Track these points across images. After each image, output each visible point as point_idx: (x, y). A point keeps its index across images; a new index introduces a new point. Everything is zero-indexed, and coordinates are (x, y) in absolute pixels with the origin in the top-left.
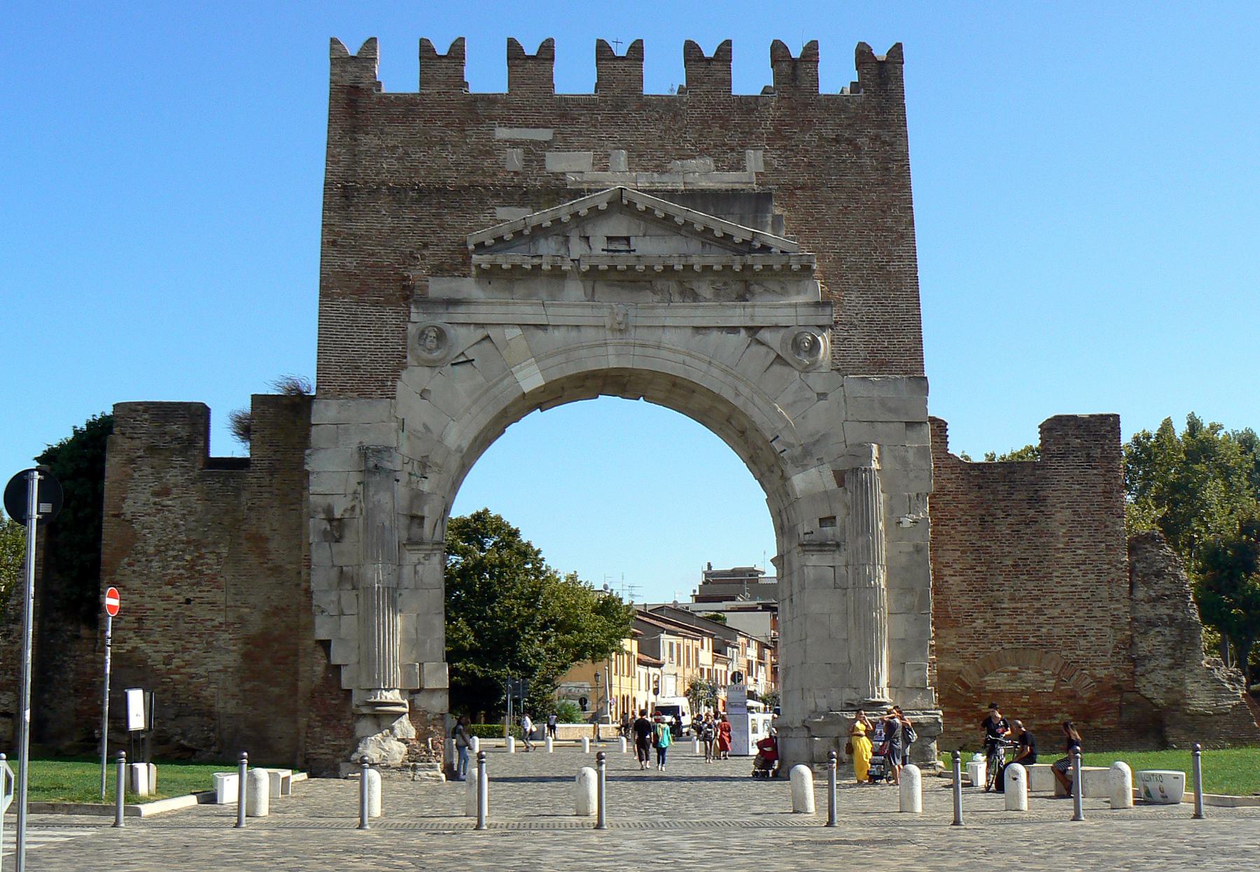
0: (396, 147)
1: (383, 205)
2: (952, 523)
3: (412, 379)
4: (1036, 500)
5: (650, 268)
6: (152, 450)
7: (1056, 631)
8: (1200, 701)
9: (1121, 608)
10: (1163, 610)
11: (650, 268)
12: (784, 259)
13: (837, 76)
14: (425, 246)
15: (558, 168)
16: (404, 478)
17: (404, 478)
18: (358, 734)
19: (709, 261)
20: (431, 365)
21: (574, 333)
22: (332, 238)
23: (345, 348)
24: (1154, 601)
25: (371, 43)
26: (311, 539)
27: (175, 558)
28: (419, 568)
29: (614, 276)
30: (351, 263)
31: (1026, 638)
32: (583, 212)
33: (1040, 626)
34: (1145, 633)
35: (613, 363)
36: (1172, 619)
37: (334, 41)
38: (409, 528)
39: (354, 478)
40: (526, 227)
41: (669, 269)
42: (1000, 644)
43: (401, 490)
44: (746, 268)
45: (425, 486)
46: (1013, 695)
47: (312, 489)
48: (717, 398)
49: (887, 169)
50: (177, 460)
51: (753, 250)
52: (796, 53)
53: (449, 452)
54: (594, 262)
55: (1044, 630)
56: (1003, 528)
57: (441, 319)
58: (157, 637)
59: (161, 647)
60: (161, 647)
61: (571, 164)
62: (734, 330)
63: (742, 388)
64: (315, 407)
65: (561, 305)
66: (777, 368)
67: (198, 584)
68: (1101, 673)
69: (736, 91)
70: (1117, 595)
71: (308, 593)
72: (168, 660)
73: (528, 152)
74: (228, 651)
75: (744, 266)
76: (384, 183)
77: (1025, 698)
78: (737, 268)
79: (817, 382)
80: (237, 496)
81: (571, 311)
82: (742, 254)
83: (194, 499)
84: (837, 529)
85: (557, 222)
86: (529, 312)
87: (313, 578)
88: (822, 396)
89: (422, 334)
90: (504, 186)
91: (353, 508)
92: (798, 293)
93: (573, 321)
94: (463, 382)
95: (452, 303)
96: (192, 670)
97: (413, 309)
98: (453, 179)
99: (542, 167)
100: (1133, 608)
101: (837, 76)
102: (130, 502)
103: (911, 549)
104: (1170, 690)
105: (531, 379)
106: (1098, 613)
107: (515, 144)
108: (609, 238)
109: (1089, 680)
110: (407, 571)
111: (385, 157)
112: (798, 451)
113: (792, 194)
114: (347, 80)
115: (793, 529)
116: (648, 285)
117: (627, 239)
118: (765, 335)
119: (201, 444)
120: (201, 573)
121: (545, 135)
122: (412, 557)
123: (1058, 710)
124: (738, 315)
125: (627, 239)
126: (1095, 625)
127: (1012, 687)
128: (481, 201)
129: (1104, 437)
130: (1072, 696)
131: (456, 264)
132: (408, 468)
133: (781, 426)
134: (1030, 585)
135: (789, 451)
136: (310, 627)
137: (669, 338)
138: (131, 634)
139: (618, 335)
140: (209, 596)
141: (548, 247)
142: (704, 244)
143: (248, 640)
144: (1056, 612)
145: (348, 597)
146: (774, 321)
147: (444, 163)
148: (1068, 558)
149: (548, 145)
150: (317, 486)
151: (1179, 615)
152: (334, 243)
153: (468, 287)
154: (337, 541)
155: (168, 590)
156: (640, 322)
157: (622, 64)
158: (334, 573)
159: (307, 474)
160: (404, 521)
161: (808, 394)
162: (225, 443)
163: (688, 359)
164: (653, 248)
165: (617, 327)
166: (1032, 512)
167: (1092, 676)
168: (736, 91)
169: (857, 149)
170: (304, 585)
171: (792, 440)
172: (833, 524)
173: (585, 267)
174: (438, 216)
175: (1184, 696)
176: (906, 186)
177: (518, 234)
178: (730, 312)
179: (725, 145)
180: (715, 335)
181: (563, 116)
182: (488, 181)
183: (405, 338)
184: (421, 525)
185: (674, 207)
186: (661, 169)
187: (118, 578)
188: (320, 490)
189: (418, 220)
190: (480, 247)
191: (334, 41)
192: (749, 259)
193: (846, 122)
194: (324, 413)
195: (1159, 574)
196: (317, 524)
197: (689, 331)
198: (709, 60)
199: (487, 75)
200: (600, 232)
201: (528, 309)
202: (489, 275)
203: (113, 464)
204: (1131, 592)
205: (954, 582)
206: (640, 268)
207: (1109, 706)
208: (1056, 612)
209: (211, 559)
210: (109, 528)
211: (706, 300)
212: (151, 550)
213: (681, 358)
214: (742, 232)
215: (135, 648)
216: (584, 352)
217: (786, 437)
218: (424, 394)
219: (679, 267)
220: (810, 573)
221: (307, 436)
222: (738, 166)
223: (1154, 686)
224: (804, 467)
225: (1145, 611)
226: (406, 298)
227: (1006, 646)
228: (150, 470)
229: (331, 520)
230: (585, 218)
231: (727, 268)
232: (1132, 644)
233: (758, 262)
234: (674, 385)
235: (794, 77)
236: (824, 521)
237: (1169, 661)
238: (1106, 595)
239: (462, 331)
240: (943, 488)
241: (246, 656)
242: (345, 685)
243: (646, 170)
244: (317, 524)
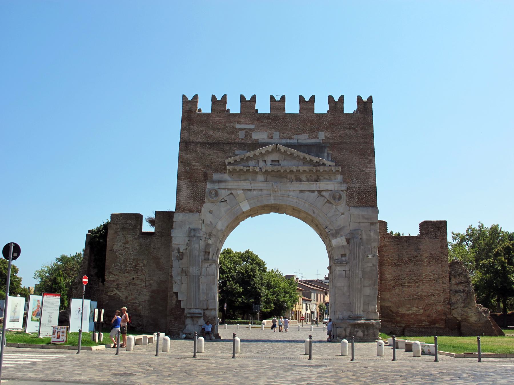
0: (203, 130)
1: (199, 149)
2: (388, 256)
3: (207, 206)
4: (417, 249)
5: (285, 171)
6: (123, 229)
7: (424, 294)
8: (473, 318)
9: (446, 286)
10: (461, 287)
11: (285, 171)
12: (330, 168)
13: (350, 107)
14: (212, 163)
15: (256, 138)
16: (203, 239)
17: (203, 239)
18: (186, 323)
19: (305, 168)
20: (213, 202)
21: (260, 192)
22: (181, 160)
23: (185, 196)
24: (458, 284)
25: (196, 97)
26: (173, 259)
27: (130, 264)
28: (208, 269)
30: (188, 168)
31: (413, 296)
32: (264, 152)
33: (418, 292)
34: (455, 295)
35: (273, 202)
36: (464, 291)
37: (184, 96)
38: (204, 256)
39: (187, 239)
41: (291, 171)
42: (404, 298)
43: (202, 243)
44: (317, 171)
45: (210, 242)
46: (408, 315)
47: (173, 242)
48: (307, 214)
49: (366, 138)
50: (131, 232)
51: (320, 165)
52: (336, 99)
53: (218, 231)
54: (267, 168)
55: (419, 293)
56: (406, 258)
57: (216, 186)
58: (123, 290)
59: (124, 293)
60: (124, 293)
61: (260, 136)
62: (313, 191)
63: (315, 211)
64: (175, 215)
66: (327, 204)
67: (137, 273)
68: (439, 308)
69: (315, 112)
70: (445, 282)
71: (171, 276)
72: (126, 298)
73: (246, 132)
74: (146, 295)
75: (317, 171)
76: (199, 142)
77: (413, 316)
78: (314, 171)
80: (150, 244)
82: (316, 166)
83: (136, 245)
84: (347, 258)
85: (255, 155)
86: (246, 185)
87: (173, 272)
88: (342, 214)
89: (210, 192)
90: (238, 143)
91: (186, 249)
92: (335, 179)
93: (260, 188)
94: (223, 208)
95: (220, 181)
96: (134, 301)
97: (207, 183)
98: (221, 140)
99: (251, 137)
100: (450, 286)
101: (350, 107)
102: (115, 246)
103: (371, 265)
104: (462, 315)
105: (245, 207)
106: (439, 288)
107: (242, 129)
108: (272, 161)
109: (435, 311)
110: (204, 270)
111: (199, 134)
112: (334, 232)
113: (334, 146)
114: (188, 108)
115: (333, 258)
117: (278, 161)
118: (324, 193)
119: (139, 227)
120: (138, 269)
121: (252, 127)
122: (205, 265)
123: (424, 320)
124: (314, 186)
125: (278, 161)
126: (437, 292)
127: (408, 312)
128: (230, 148)
129: (441, 228)
130: (429, 316)
131: (222, 170)
132: (205, 236)
134: (415, 278)
135: (331, 232)
136: (172, 288)
137: (291, 193)
138: (115, 289)
139: (275, 193)
140: (140, 277)
141: (252, 163)
142: (304, 163)
143: (152, 291)
144: (424, 287)
145: (184, 278)
146: (327, 188)
147: (219, 136)
148: (428, 269)
149: (252, 130)
150: (174, 241)
151: (467, 289)
152: (182, 162)
153: (226, 176)
154: (181, 259)
155: (127, 275)
157: (278, 103)
158: (180, 270)
159: (172, 237)
160: (203, 253)
161: (338, 213)
162: (147, 228)
164: (287, 165)
166: (415, 253)
167: (436, 309)
168: (316, 112)
169: (357, 131)
170: (170, 274)
171: (332, 228)
172: (345, 257)
173: (264, 170)
174: (216, 153)
175: (468, 317)
176: (373, 144)
177: (242, 159)
178: (312, 186)
179: (312, 130)
180: (307, 193)
181: (258, 120)
182: (233, 141)
183: (205, 193)
184: (209, 255)
185: (293, 151)
186: (291, 138)
187: (111, 271)
188: (176, 243)
189: (210, 154)
190: (230, 164)
191: (184, 96)
192: (318, 168)
193: (353, 122)
194: (177, 218)
195: (459, 275)
196: (175, 254)
198: (307, 102)
199: (234, 107)
200: (269, 159)
201: (244, 184)
202: (232, 172)
203: (110, 233)
204: (450, 281)
205: (388, 276)
206: (282, 171)
207: (442, 320)
208: (424, 287)
209: (141, 265)
210: (108, 255)
212: (122, 262)
214: (316, 159)
215: (116, 294)
218: (210, 212)
220: (337, 273)
221: (173, 225)
222: (316, 137)
223: (457, 314)
224: (336, 237)
225: (455, 287)
226: (205, 180)
227: (406, 298)
228: (122, 236)
229: (179, 252)
230: (264, 154)
231: (311, 171)
232: (450, 298)
233: (321, 169)
234: (294, 209)
235: (335, 107)
236: (342, 256)
237: (463, 305)
238: (441, 282)
239: (223, 191)
240: (385, 245)
241: (152, 297)
242: (182, 307)
243: (285, 138)
244: (175, 254)
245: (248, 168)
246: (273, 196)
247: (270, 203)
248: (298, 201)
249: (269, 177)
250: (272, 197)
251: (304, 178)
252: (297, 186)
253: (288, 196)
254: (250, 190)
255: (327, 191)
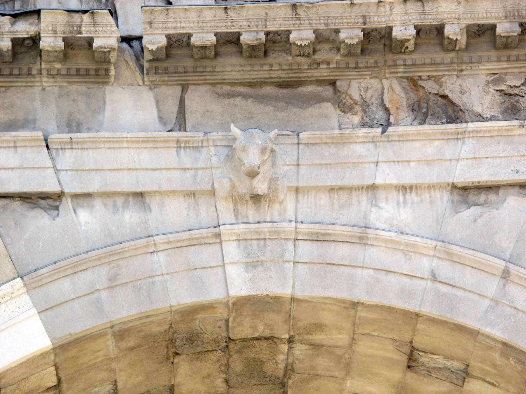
29: (232, 67)
35: (240, 284)
65: (95, 144)
81: (126, 157)
93: (126, 183)
116: (328, 91)
139: (250, 212)
156: (306, 177)
165: (243, 189)
173: (155, 41)
197: (443, 199)
206: (302, 36)
211: (480, 118)
219: (404, 32)
245: (24, 28)
246: (240, 240)
247: (214, 293)
248: (445, 269)
249: (198, 100)
250: (232, 251)
251: (474, 89)
252: (427, 154)
253: (362, 237)
254: (46, 201)
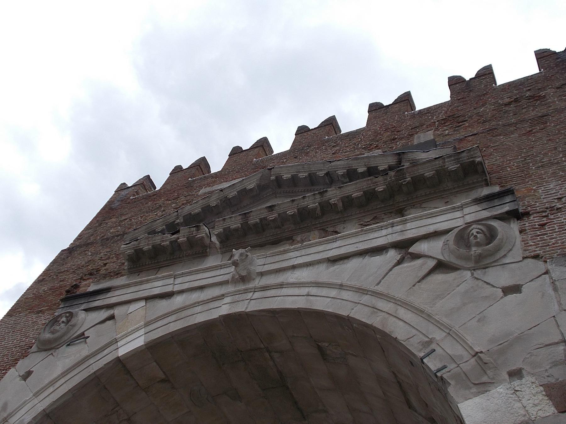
40: (178, 218)
66: (439, 278)
79: (501, 277)
112: (469, 365)
133: (438, 335)
146: (432, 229)
163: (314, 291)
213: (304, 291)
216: (198, 309)
217: (451, 348)
224: (483, 387)
255: (436, 234)
